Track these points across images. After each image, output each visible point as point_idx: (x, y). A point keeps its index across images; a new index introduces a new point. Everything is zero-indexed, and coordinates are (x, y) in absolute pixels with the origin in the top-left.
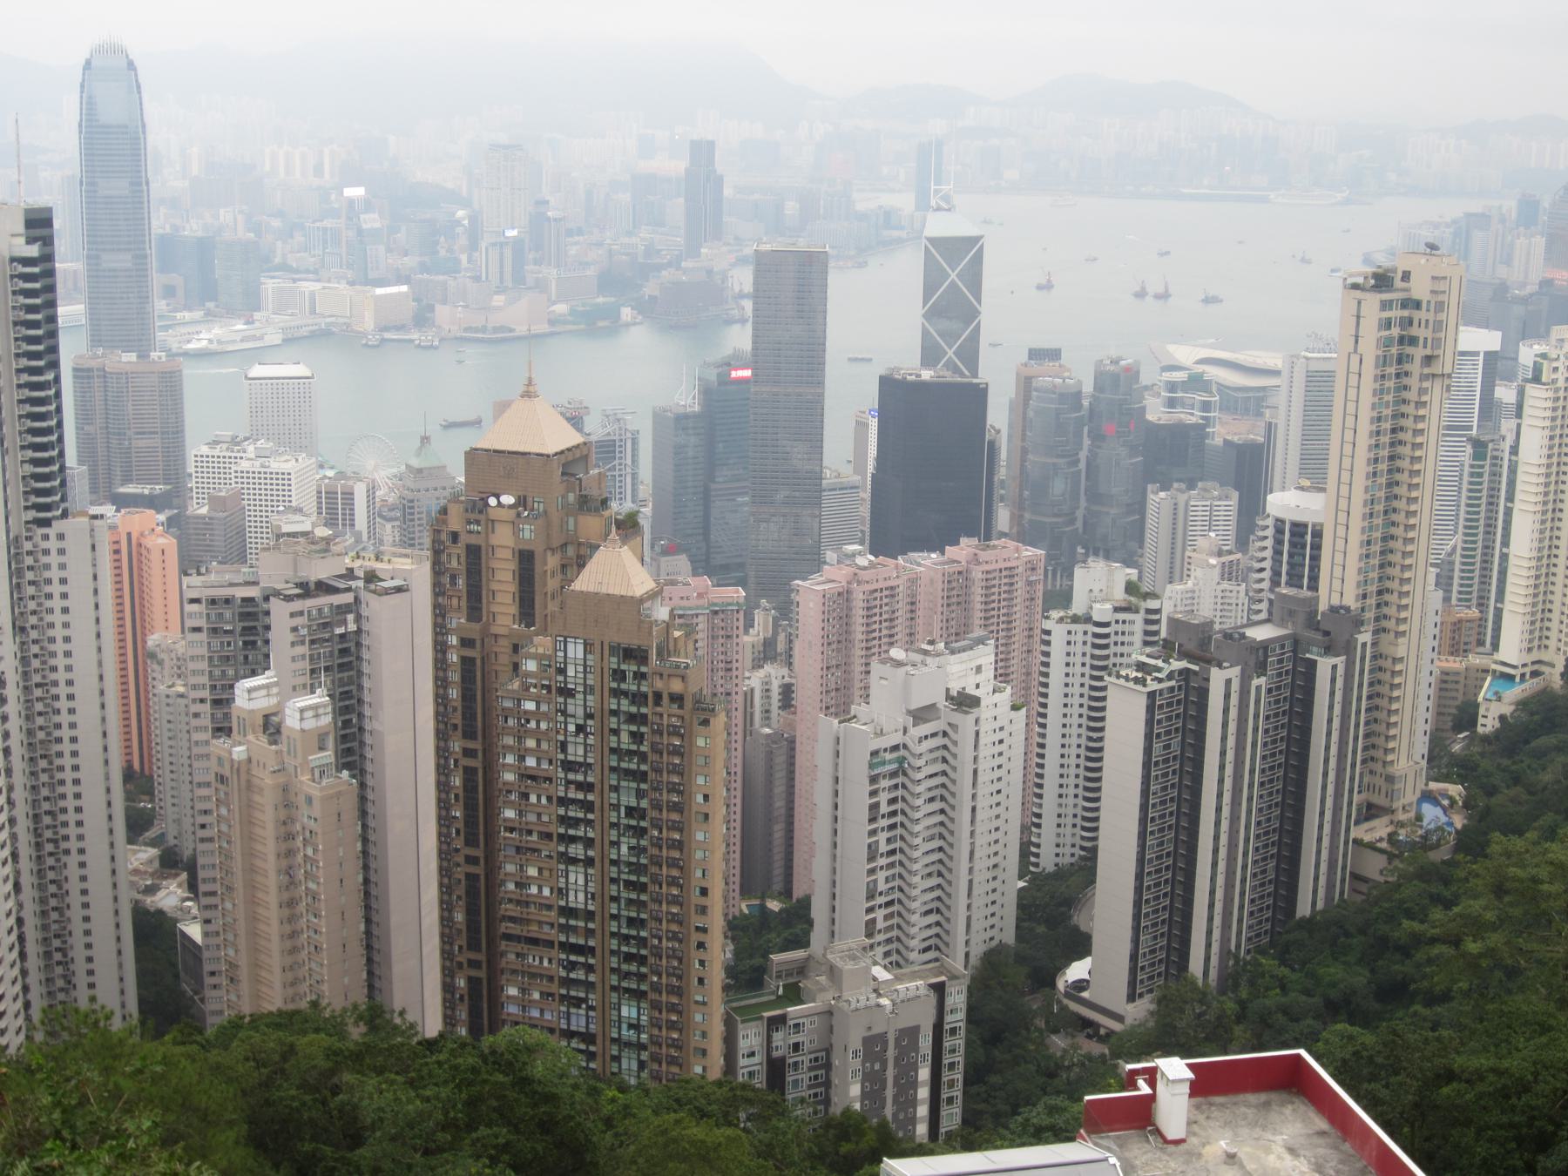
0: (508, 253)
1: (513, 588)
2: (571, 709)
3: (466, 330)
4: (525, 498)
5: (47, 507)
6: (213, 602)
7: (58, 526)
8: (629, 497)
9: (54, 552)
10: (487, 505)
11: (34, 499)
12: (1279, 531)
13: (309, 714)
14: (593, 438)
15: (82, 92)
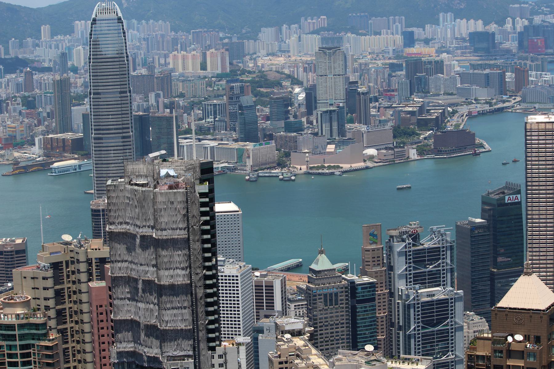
0: (335, 116)
3: (311, 168)
4: (529, 336)
8: (449, 283)
14: (426, 246)
15: (91, 38)
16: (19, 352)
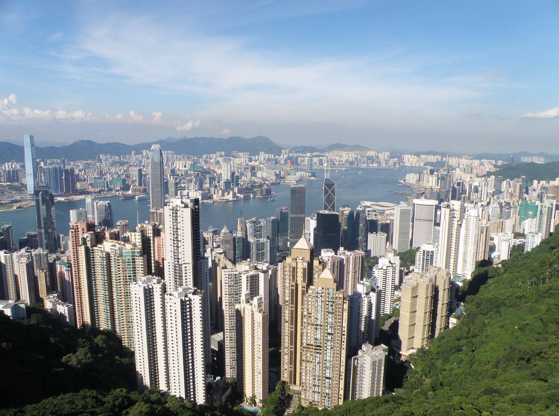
0: (227, 183)
1: (302, 275)
2: (319, 300)
5: (198, 257)
6: (229, 275)
7: (200, 261)
12: (424, 251)
16: (131, 261)
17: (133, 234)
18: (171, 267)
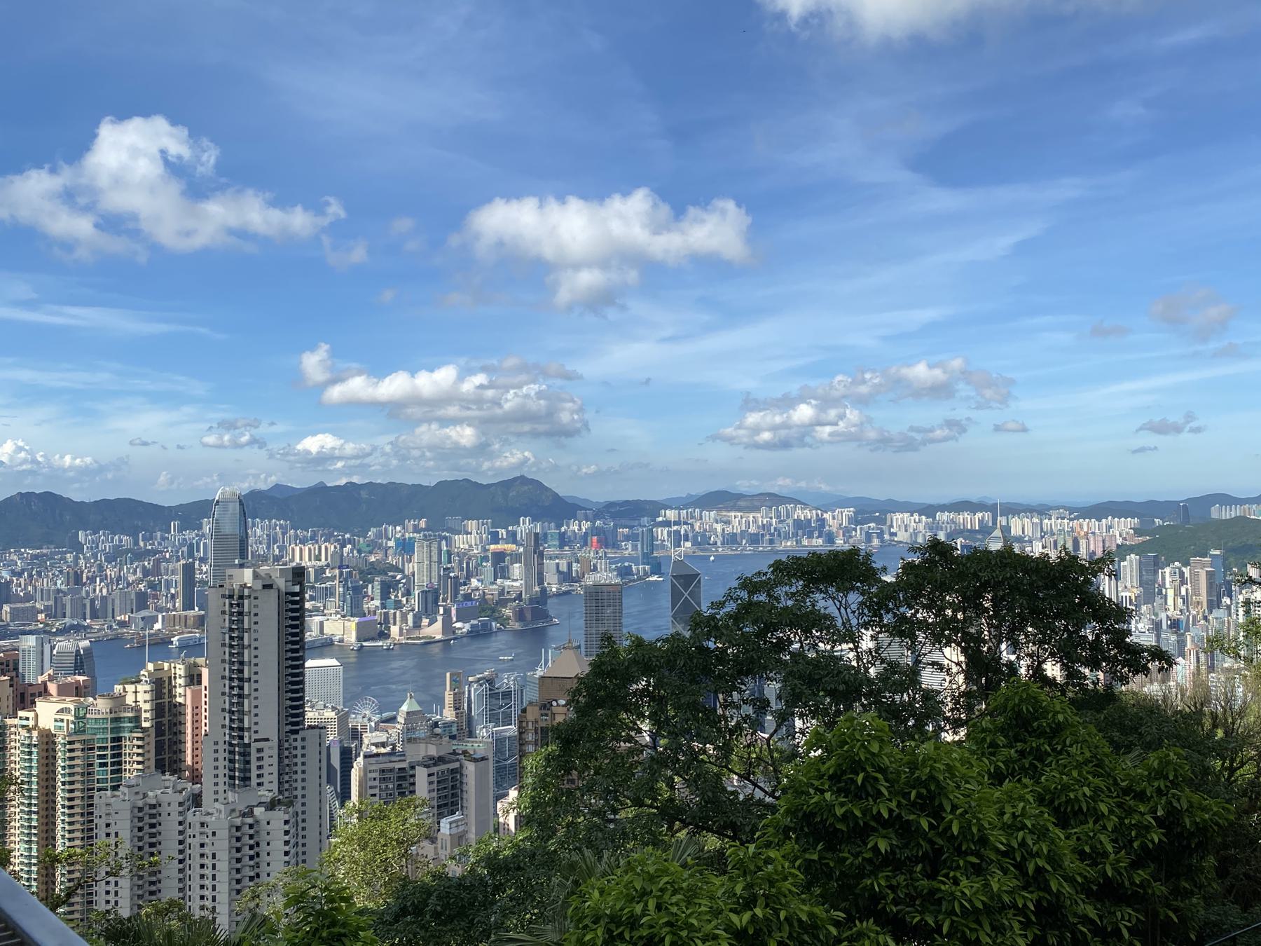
5: (297, 724)
6: (383, 771)
9: (299, 748)
10: (552, 705)
11: (290, 719)
13: (452, 826)
16: (109, 745)
17: (130, 688)
18: (222, 755)
